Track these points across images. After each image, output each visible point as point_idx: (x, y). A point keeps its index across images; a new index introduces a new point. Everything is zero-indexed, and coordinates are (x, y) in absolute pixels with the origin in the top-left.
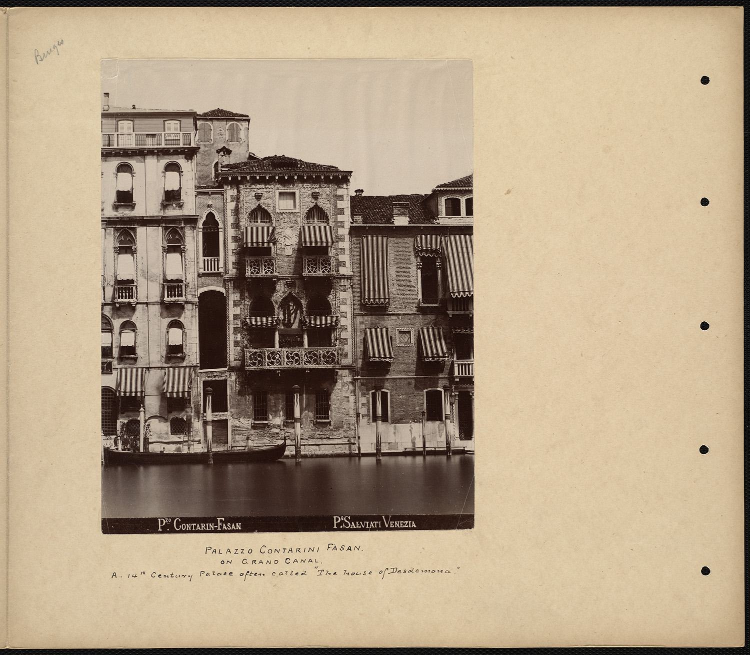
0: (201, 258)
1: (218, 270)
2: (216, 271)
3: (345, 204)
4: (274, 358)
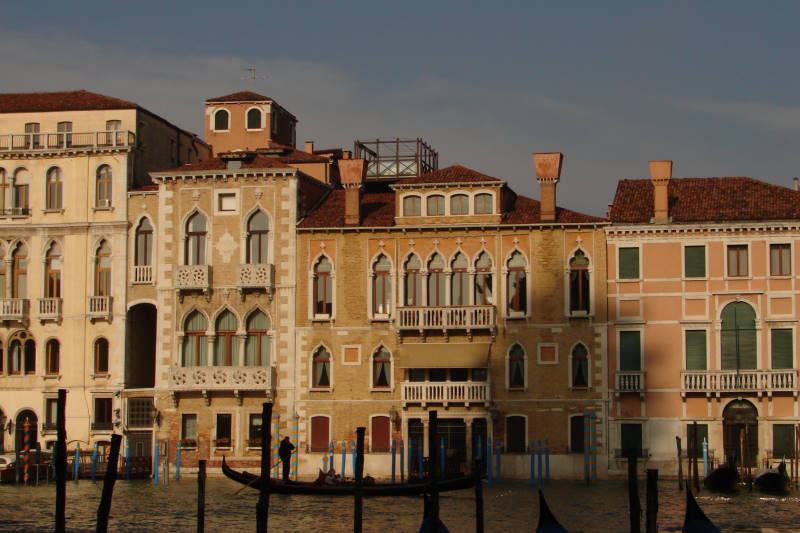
0: (133, 267)
3: (291, 206)
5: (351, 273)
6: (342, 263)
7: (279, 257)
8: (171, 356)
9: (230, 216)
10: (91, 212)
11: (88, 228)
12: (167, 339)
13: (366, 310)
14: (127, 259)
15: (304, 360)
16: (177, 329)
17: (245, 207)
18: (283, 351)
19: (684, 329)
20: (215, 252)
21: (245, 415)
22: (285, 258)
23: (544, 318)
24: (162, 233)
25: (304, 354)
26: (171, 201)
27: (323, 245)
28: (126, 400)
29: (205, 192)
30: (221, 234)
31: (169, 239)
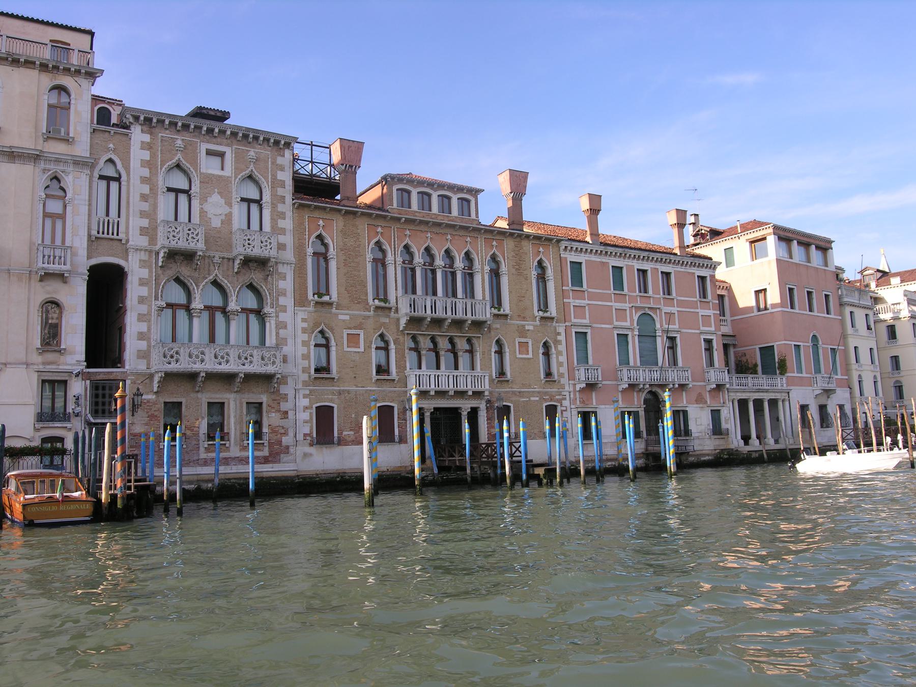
2: (115, 236)
3: (286, 177)
5: (351, 256)
6: (341, 243)
7: (277, 230)
8: (149, 329)
10: (41, 141)
11: (36, 158)
12: (144, 309)
13: (367, 295)
14: (90, 205)
15: (305, 344)
16: (156, 299)
17: (237, 170)
18: (281, 331)
19: (616, 332)
20: (203, 213)
21: (241, 403)
22: (283, 231)
23: (519, 316)
24: (135, 180)
25: (305, 337)
26: (145, 146)
27: (321, 222)
28: (88, 382)
30: (210, 194)
31: (146, 189)
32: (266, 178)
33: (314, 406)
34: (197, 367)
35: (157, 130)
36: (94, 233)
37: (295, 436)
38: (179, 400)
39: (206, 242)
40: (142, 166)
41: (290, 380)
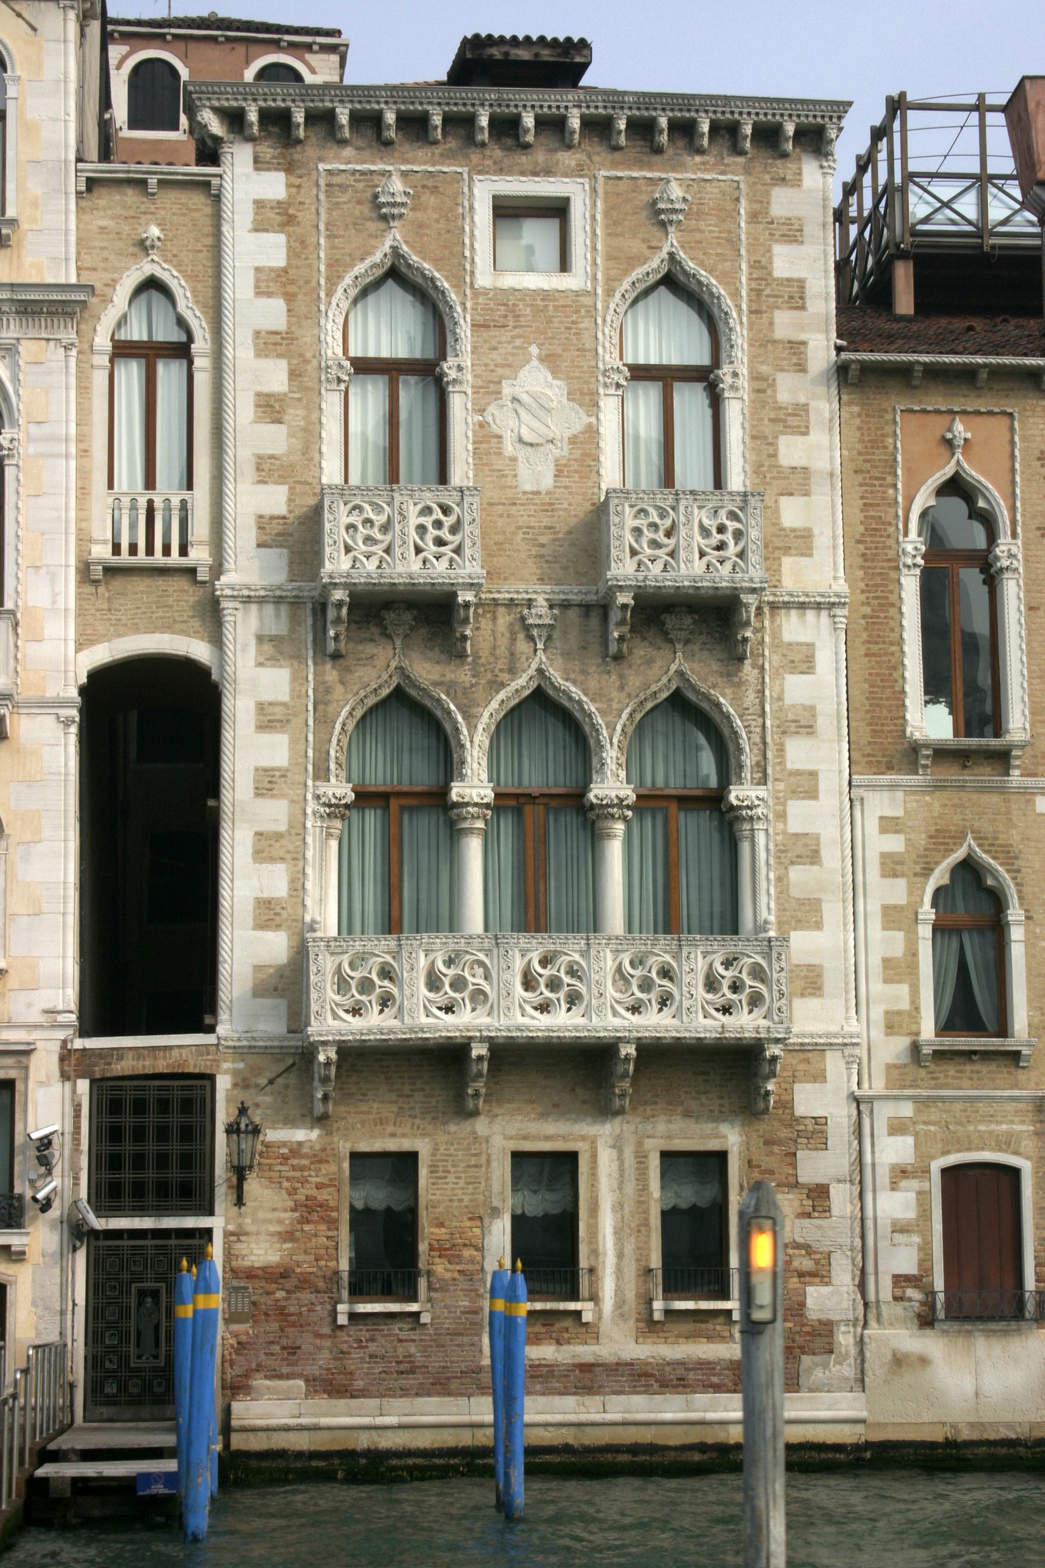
1: (183, 552)
2: (175, 558)
3: (811, 264)
4: (458, 984)
7: (778, 479)
9: (546, 295)
12: (275, 814)
14: (84, 453)
16: (322, 773)
18: (797, 874)
21: (641, 1157)
22: (798, 482)
24: (240, 350)
25: (898, 891)
28: (83, 1086)
29: (432, 184)
30: (512, 367)
31: (275, 376)
32: (730, 279)
33: (937, 1166)
34: (466, 1022)
35: (311, 151)
36: (102, 552)
37: (862, 1286)
38: (405, 1145)
39: (489, 554)
40: (259, 293)
41: (833, 1063)
